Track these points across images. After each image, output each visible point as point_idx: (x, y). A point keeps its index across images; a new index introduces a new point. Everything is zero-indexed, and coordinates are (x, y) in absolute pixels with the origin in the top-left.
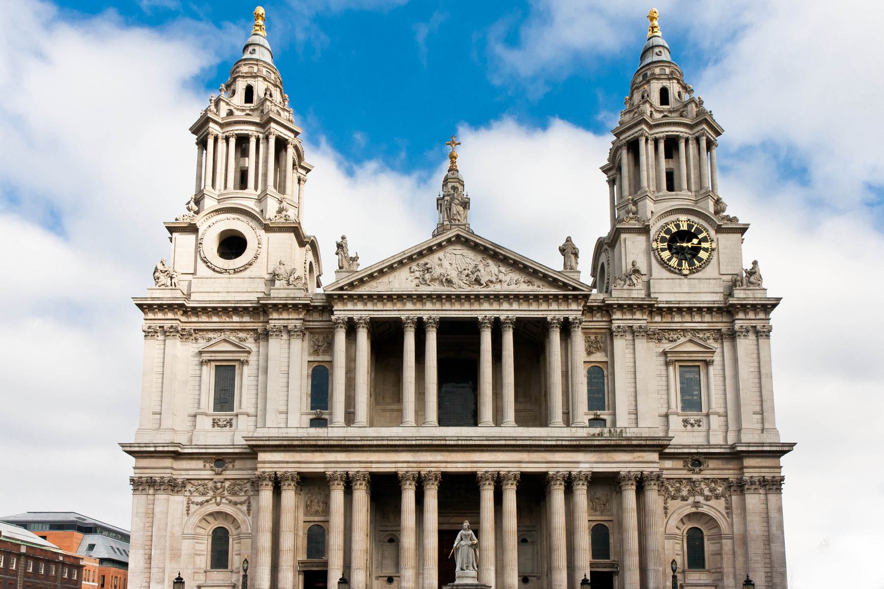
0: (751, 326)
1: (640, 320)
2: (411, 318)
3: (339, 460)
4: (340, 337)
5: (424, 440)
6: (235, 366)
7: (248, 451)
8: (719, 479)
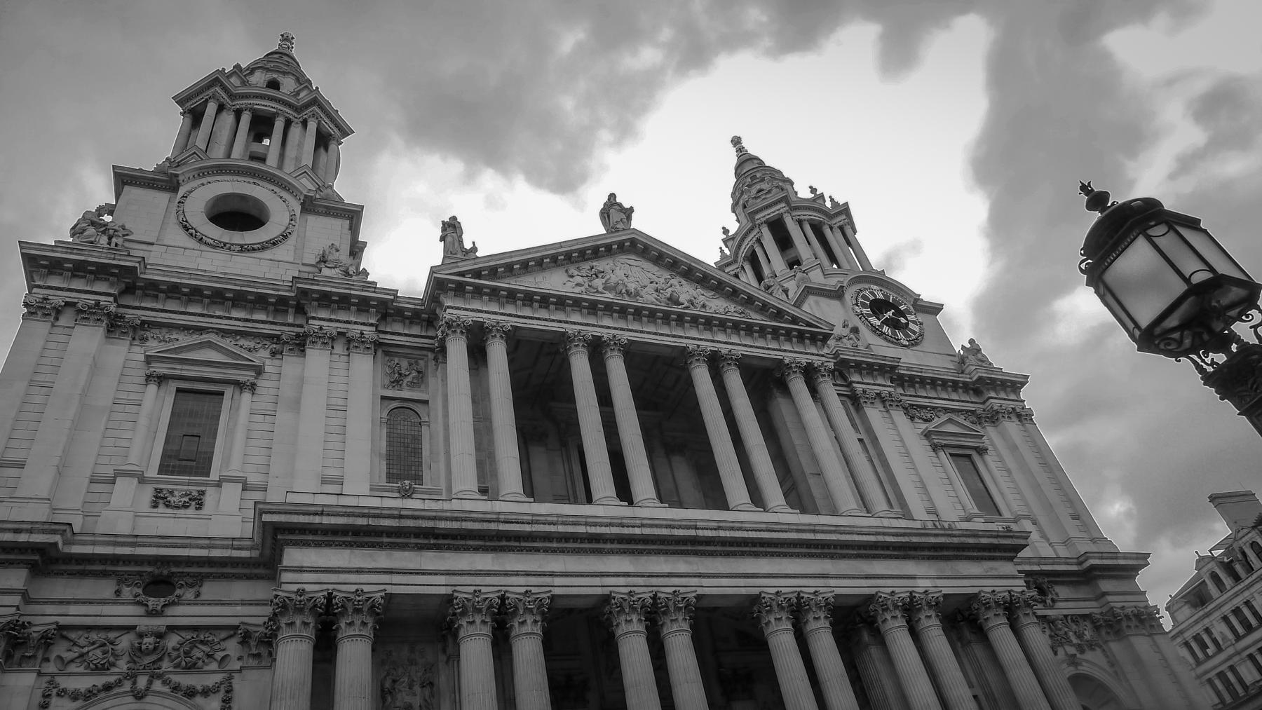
0: (1012, 408)
1: (883, 386)
2: (582, 334)
3: (480, 567)
4: (457, 350)
5: (657, 526)
6: (222, 394)
7: (245, 554)
8: (1079, 615)
